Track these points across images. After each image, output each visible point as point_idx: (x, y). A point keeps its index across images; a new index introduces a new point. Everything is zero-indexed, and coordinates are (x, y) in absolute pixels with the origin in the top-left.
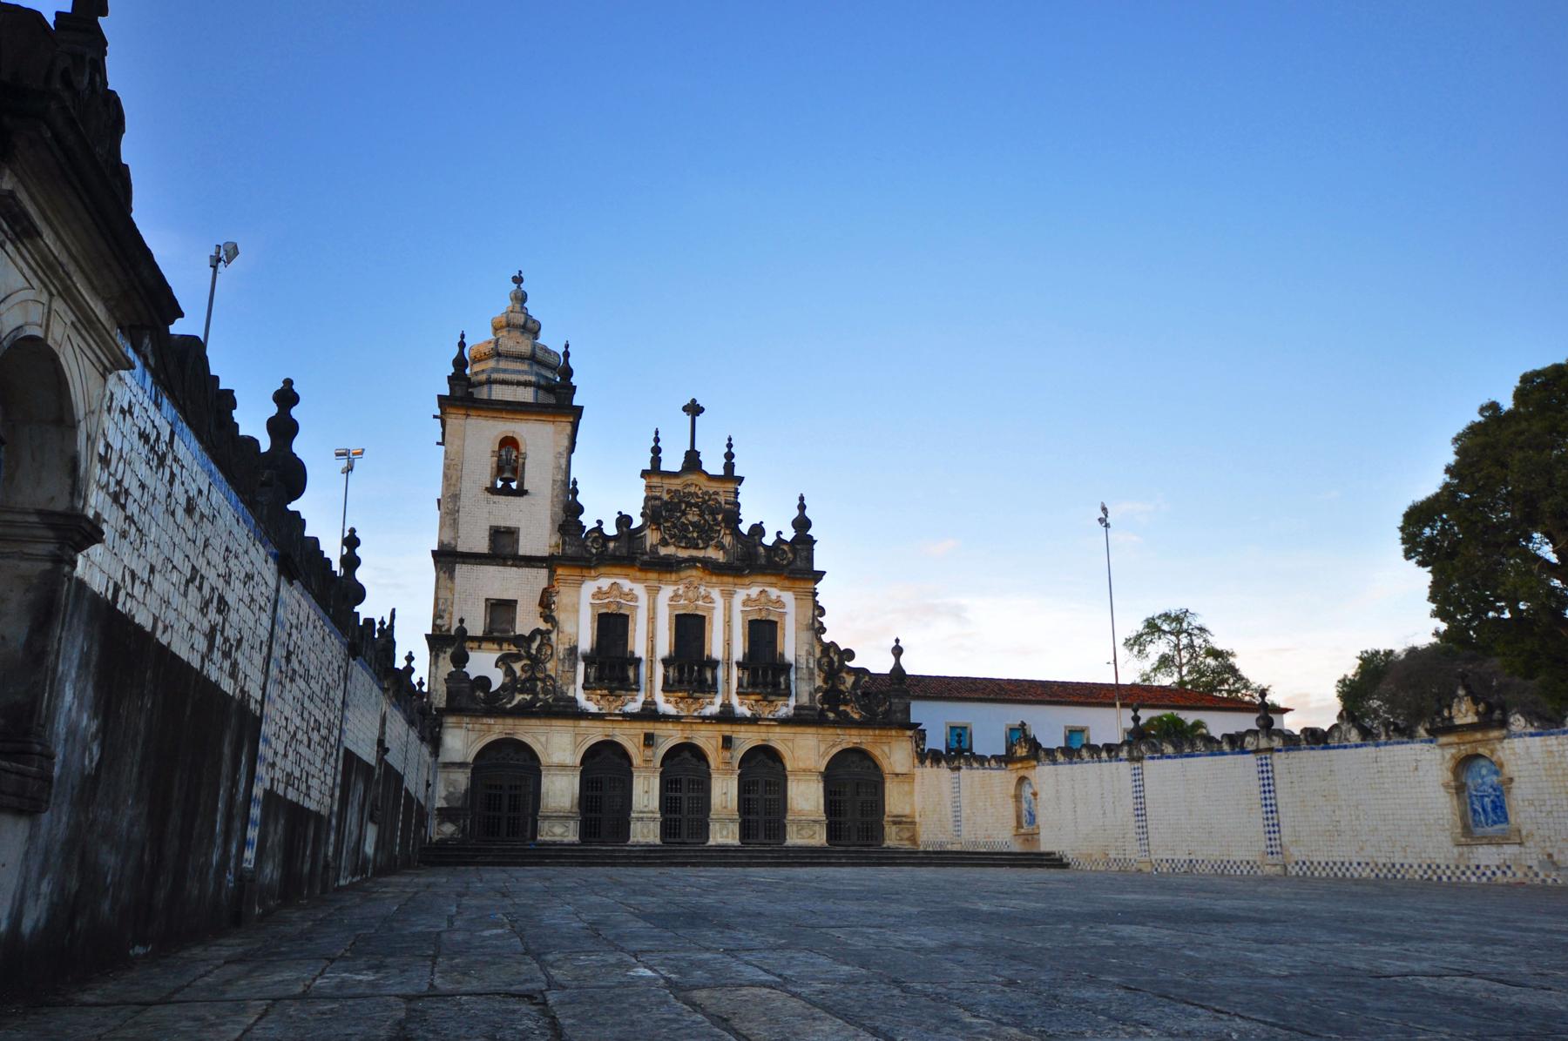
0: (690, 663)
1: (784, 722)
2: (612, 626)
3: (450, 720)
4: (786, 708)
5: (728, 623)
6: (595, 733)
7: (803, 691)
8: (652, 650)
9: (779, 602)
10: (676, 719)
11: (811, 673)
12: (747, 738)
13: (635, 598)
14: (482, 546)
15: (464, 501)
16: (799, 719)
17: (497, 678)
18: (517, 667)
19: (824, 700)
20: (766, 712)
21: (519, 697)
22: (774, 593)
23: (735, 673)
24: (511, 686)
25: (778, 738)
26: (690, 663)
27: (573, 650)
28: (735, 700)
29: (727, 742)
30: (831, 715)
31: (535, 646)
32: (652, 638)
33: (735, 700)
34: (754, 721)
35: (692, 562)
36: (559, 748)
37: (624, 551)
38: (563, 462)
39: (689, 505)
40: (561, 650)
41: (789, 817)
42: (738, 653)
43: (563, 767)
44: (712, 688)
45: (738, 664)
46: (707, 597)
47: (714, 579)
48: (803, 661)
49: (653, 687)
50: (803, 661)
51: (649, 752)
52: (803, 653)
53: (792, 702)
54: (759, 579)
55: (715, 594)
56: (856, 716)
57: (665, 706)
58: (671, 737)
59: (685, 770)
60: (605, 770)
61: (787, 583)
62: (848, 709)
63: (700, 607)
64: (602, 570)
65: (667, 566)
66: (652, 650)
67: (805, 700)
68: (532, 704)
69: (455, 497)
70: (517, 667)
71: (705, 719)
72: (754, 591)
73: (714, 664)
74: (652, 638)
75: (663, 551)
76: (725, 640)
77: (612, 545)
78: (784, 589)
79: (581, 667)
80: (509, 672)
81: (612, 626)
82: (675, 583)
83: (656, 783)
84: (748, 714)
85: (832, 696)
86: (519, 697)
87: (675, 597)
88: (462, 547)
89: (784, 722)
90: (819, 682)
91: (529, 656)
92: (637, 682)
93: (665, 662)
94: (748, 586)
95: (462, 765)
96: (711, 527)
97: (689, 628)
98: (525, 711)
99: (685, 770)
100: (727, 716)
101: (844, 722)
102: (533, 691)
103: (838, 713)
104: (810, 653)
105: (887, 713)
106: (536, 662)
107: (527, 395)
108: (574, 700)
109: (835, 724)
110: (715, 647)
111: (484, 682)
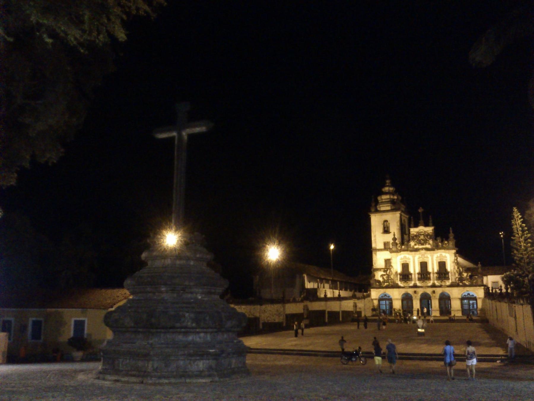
0: (424, 274)
1: (448, 286)
2: (405, 266)
3: (372, 290)
4: (448, 283)
5: (433, 264)
6: (403, 291)
7: (453, 278)
8: (415, 271)
9: (446, 257)
10: (421, 287)
11: (455, 273)
12: (439, 291)
13: (409, 259)
14: (382, 247)
15: (377, 236)
16: (452, 285)
17: (381, 279)
18: (385, 277)
19: (459, 280)
20: (443, 284)
21: (386, 284)
22: (444, 254)
23: (436, 275)
24: (384, 282)
25: (448, 290)
26: (424, 274)
27: (396, 273)
28: (436, 282)
29: (434, 292)
30: (461, 284)
31: (388, 272)
32: (415, 269)
33: (436, 282)
34: (441, 286)
35: (422, 249)
36: (396, 295)
37: (406, 249)
38: (399, 224)
39: (421, 235)
40: (394, 272)
41: (452, 309)
42: (436, 270)
43: (397, 299)
44: (429, 279)
45: (436, 273)
46: (427, 257)
47: (429, 252)
48: (452, 271)
49: (415, 280)
50: (452, 271)
51: (415, 295)
52: (452, 268)
53: (450, 281)
54: (439, 251)
55: (429, 256)
56: (467, 284)
57: (418, 284)
58: (420, 291)
59: (426, 299)
60: (407, 299)
61: (447, 251)
62: (465, 282)
63: (425, 260)
64: (402, 253)
65: (417, 250)
66: (415, 271)
67: (454, 280)
68: (389, 285)
69: (375, 236)
70: (385, 277)
71: (428, 287)
72: (438, 254)
73: (429, 273)
74: (415, 269)
75: (416, 247)
76: (433, 268)
77: (403, 247)
78: (446, 253)
79: (399, 276)
80: (383, 278)
81: (405, 266)
82: (420, 254)
83: (418, 302)
84: (439, 285)
85: (461, 279)
86: (386, 284)
87: (419, 258)
88: (378, 248)
89: (448, 286)
90: (457, 275)
91: (387, 274)
92: (412, 279)
93: (418, 274)
94: (437, 253)
95: (376, 299)
96: (427, 240)
97: (424, 265)
98: (387, 287)
99: (426, 299)
100: (434, 286)
101: (465, 286)
102: (388, 282)
103: (463, 283)
104: (454, 268)
105: (476, 282)
106: (389, 276)
107: (389, 208)
108: (398, 284)
109: (461, 286)
110: (430, 269)
111: (379, 281)
